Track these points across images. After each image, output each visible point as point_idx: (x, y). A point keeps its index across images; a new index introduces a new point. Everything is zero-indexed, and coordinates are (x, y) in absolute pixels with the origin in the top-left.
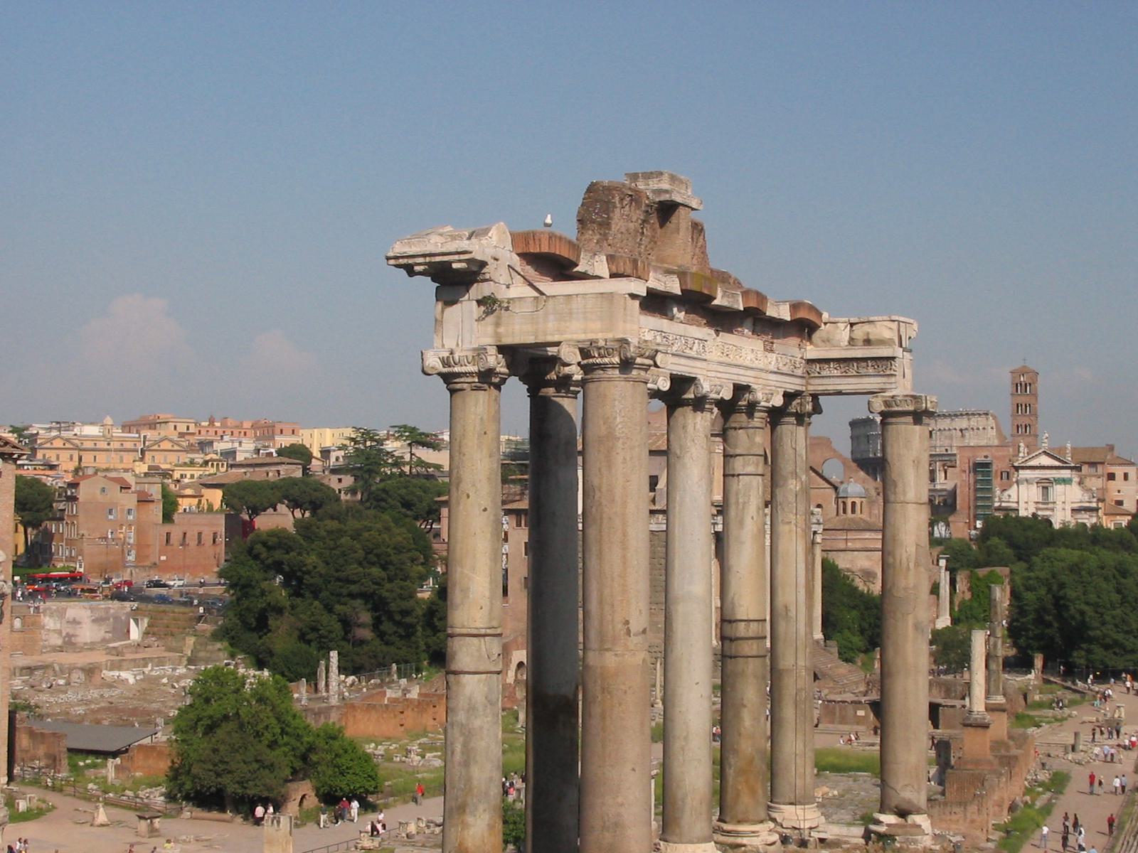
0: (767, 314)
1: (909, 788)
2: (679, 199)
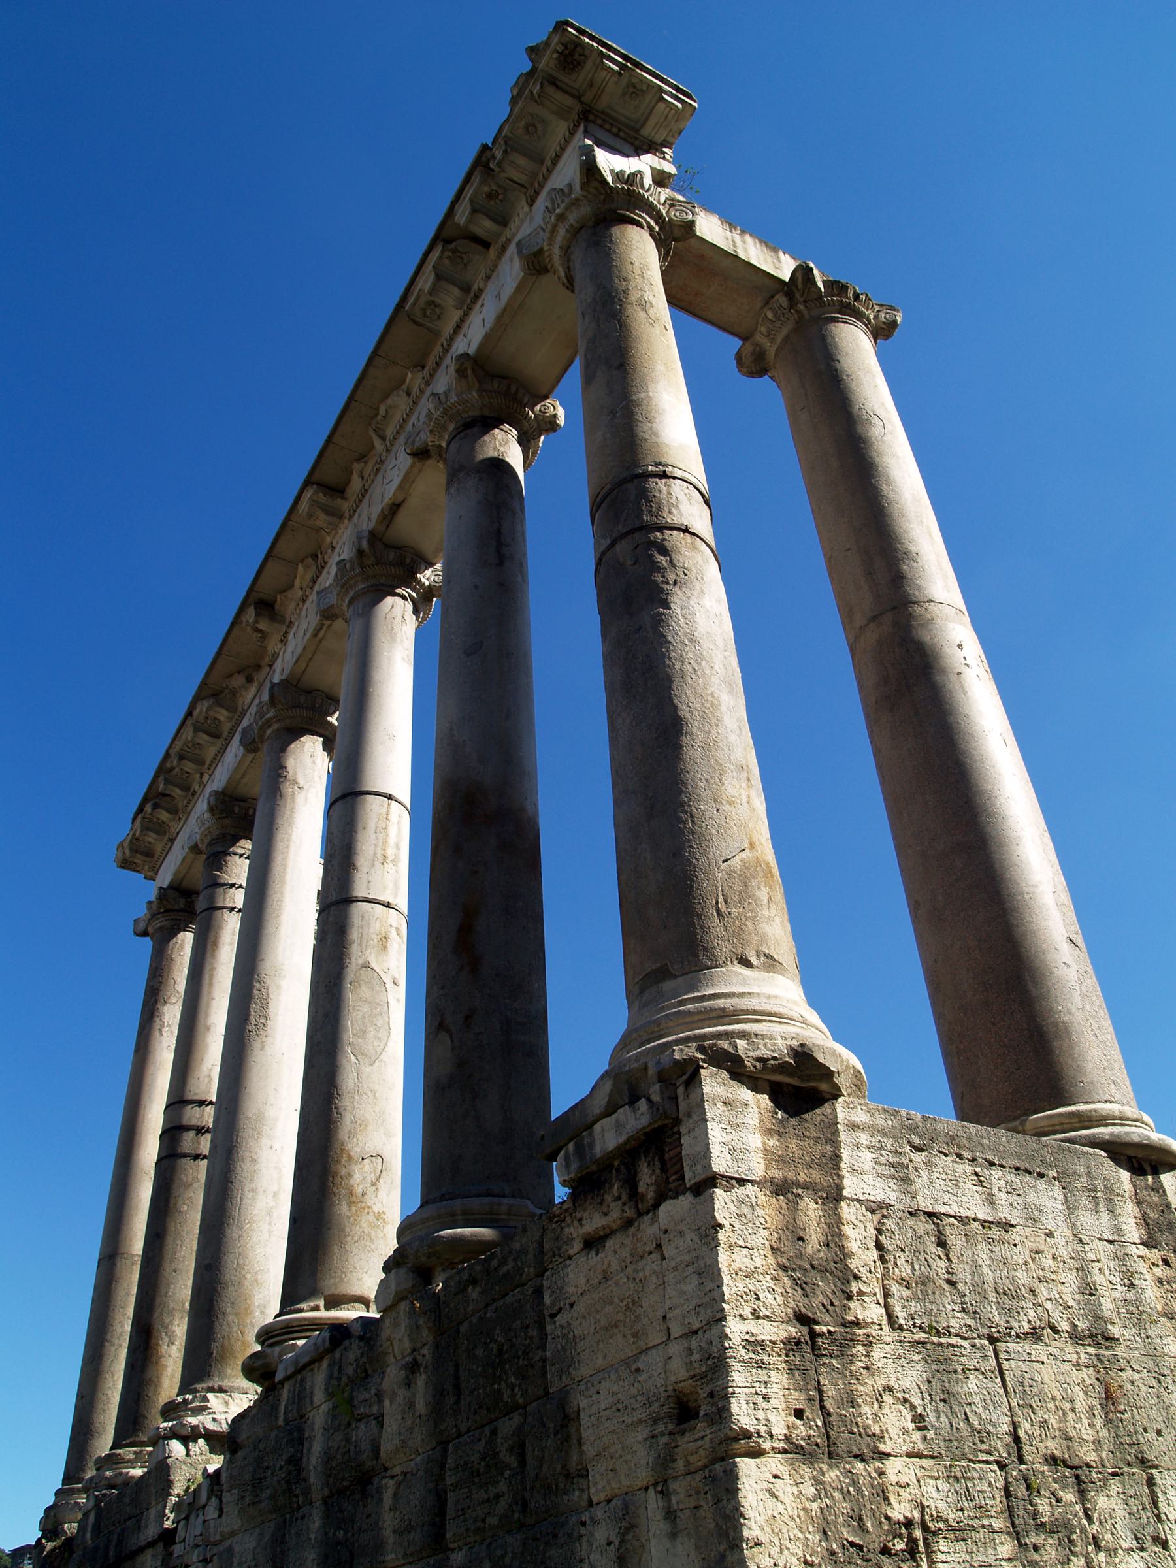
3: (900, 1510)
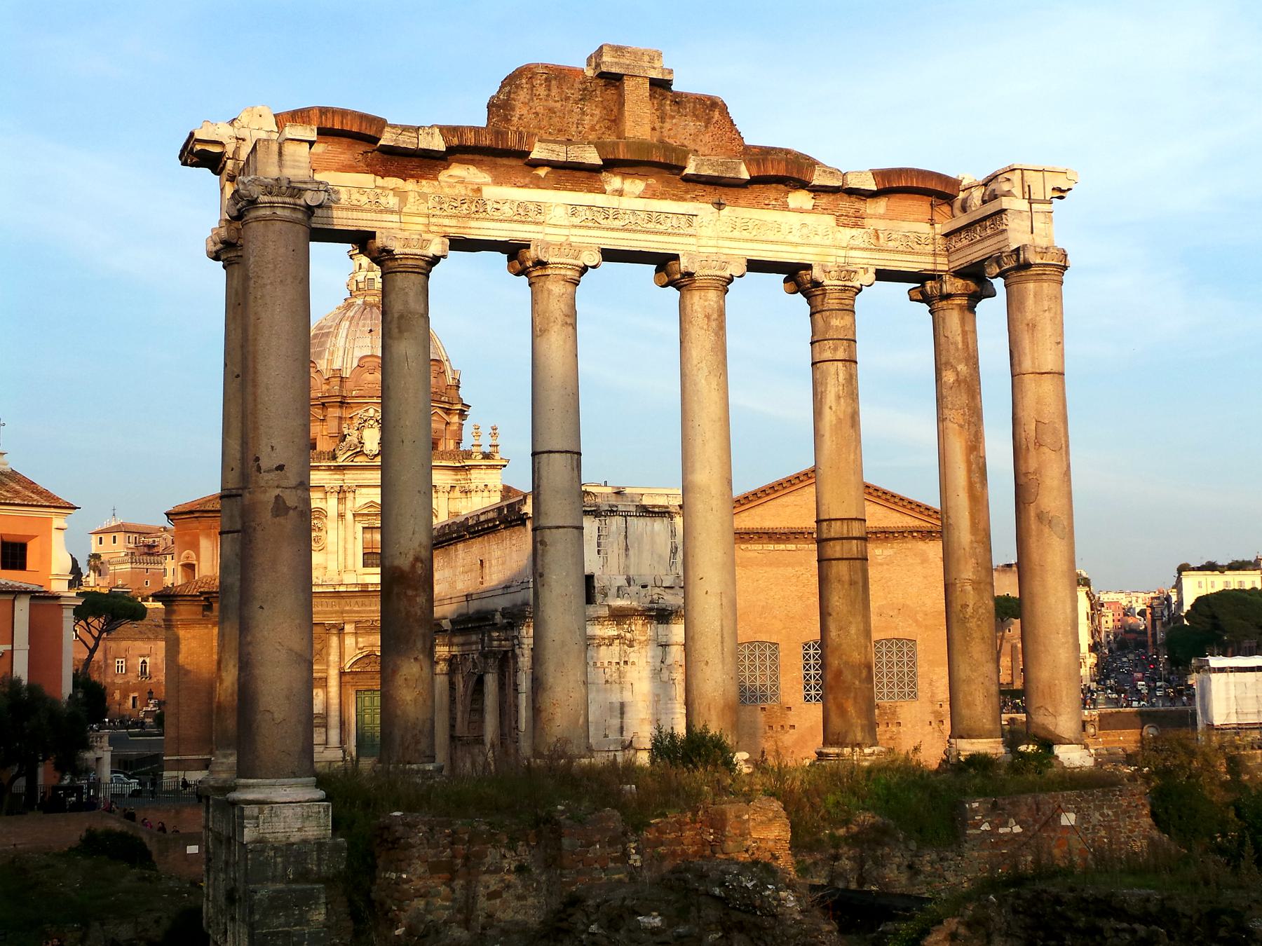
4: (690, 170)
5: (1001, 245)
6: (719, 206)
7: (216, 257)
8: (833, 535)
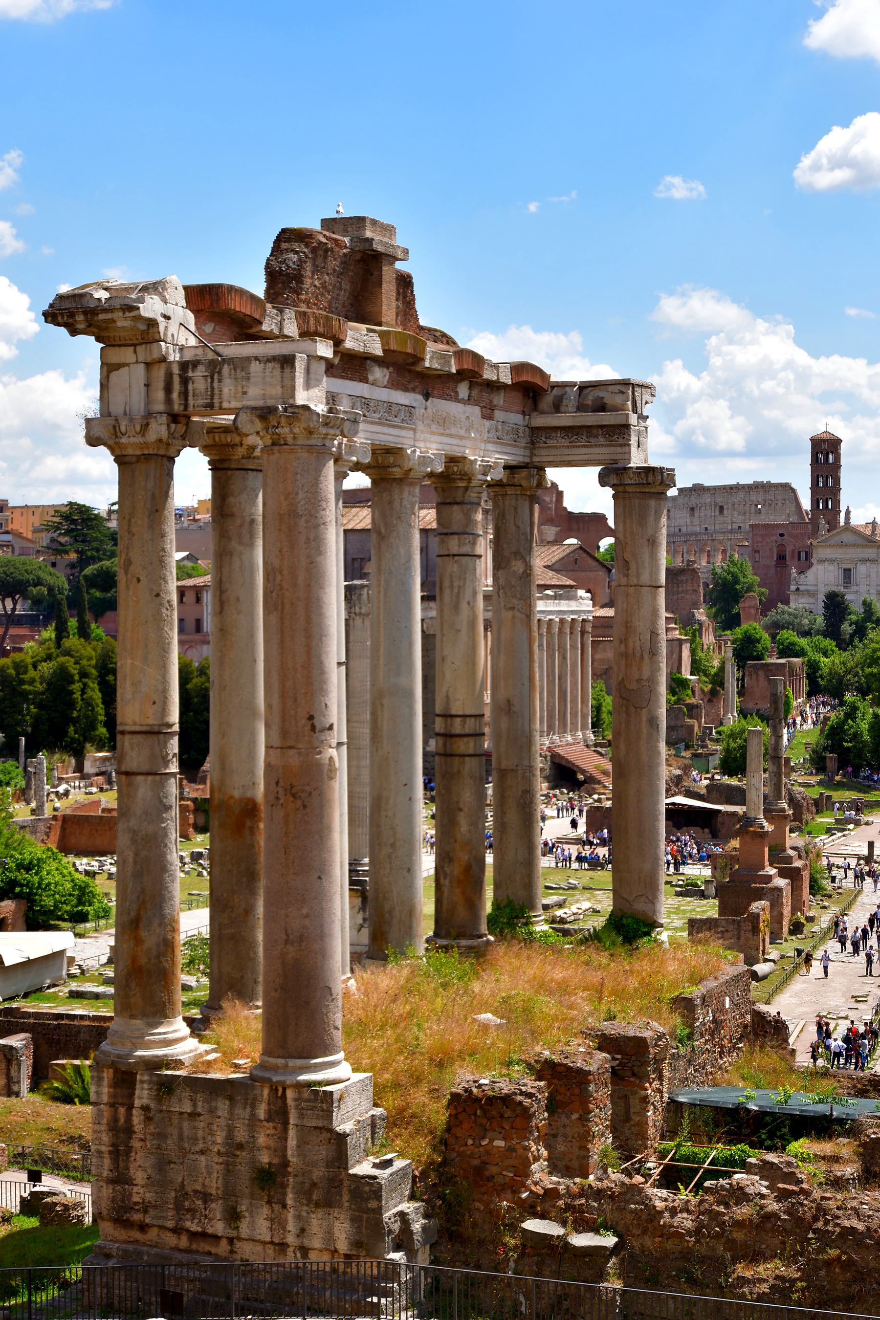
0: (485, 376)
1: (643, 899)
2: (380, 248)
3: (136, 1199)
4: (427, 364)
5: (619, 457)
6: (427, 396)
7: (92, 441)
8: (467, 731)
